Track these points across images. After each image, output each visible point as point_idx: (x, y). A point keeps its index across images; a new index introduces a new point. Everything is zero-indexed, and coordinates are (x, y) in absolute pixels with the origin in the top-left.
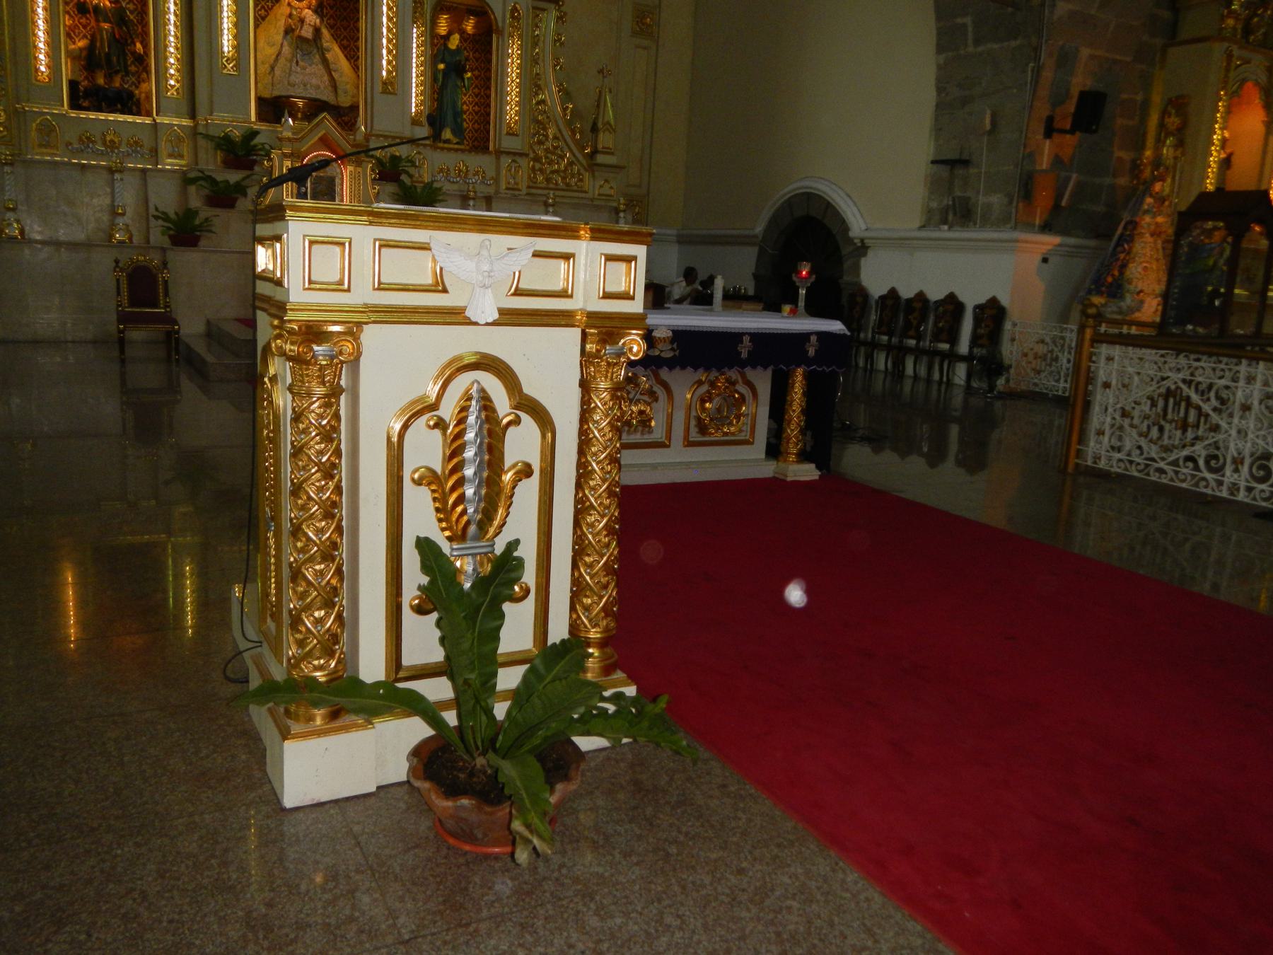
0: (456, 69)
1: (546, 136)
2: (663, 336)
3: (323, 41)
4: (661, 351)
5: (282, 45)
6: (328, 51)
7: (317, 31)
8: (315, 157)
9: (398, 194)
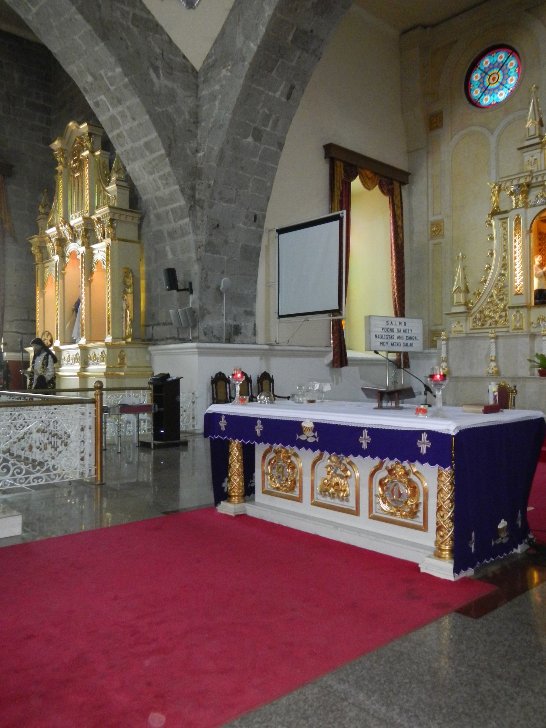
2: (308, 426)
4: (308, 437)
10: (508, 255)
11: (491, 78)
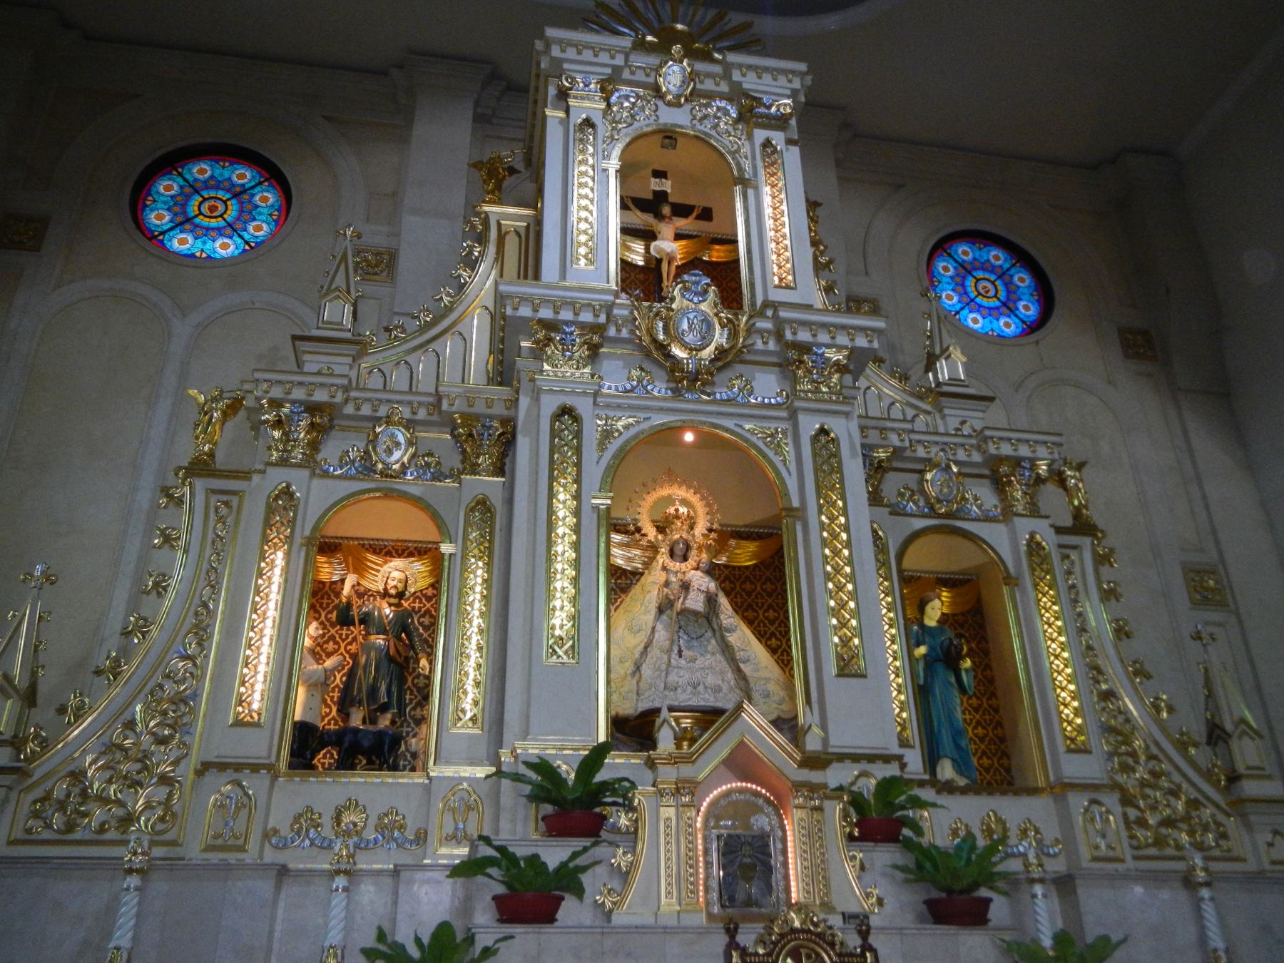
0: (949, 659)
1: (1133, 754)
3: (722, 617)
5: (653, 628)
6: (729, 631)
7: (711, 600)
8: (728, 794)
9: (903, 869)
10: (216, 602)
11: (206, 205)
